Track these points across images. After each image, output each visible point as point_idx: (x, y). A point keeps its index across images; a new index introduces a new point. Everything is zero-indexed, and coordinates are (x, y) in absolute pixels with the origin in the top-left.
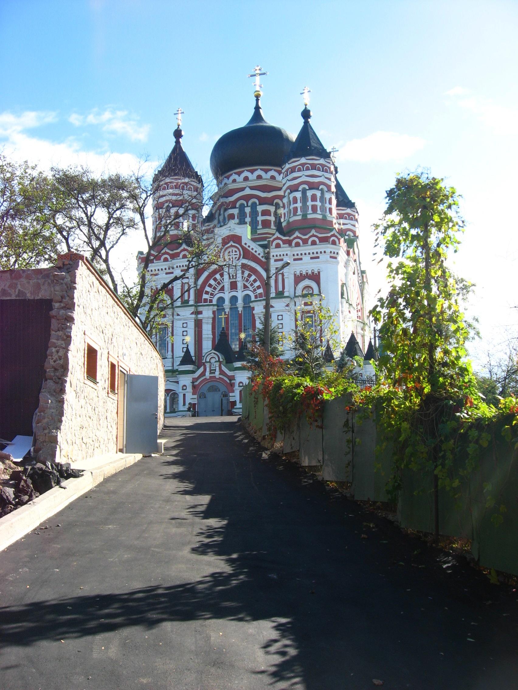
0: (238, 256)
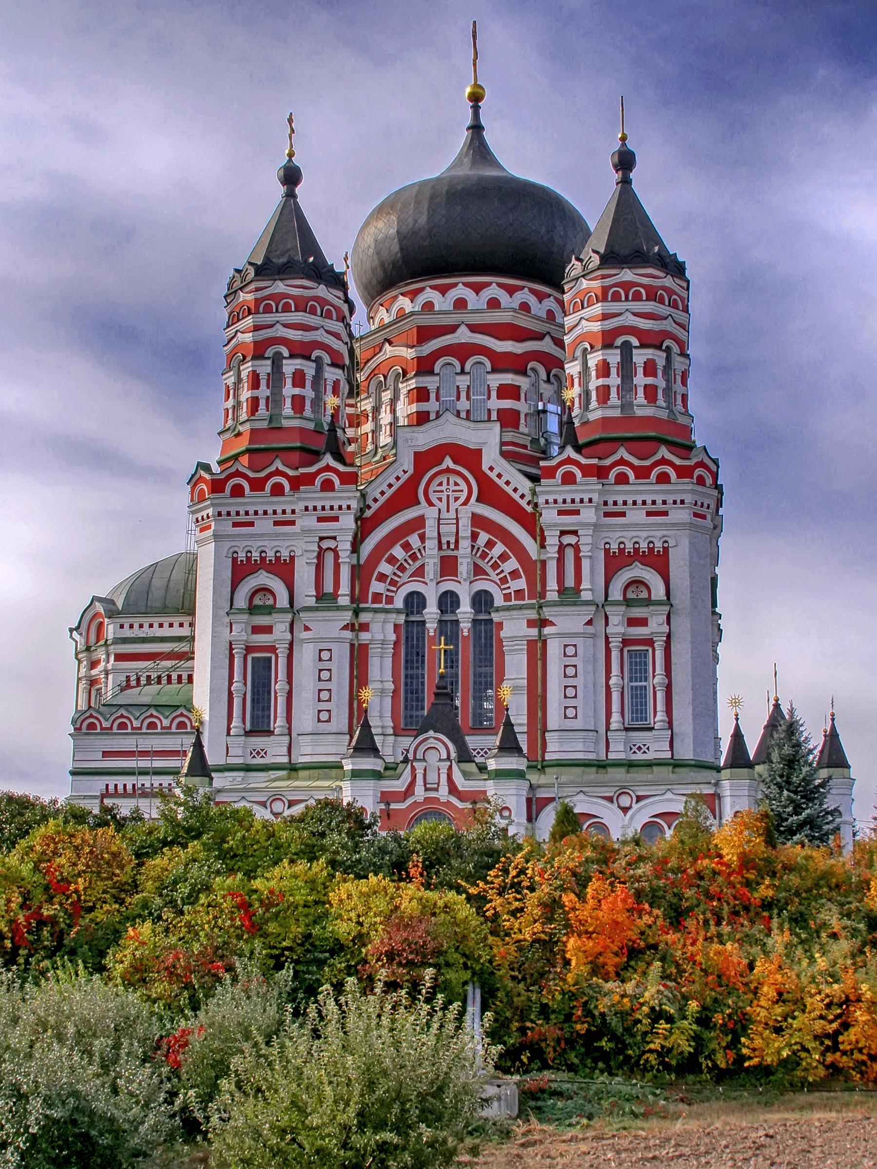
0: (463, 496)
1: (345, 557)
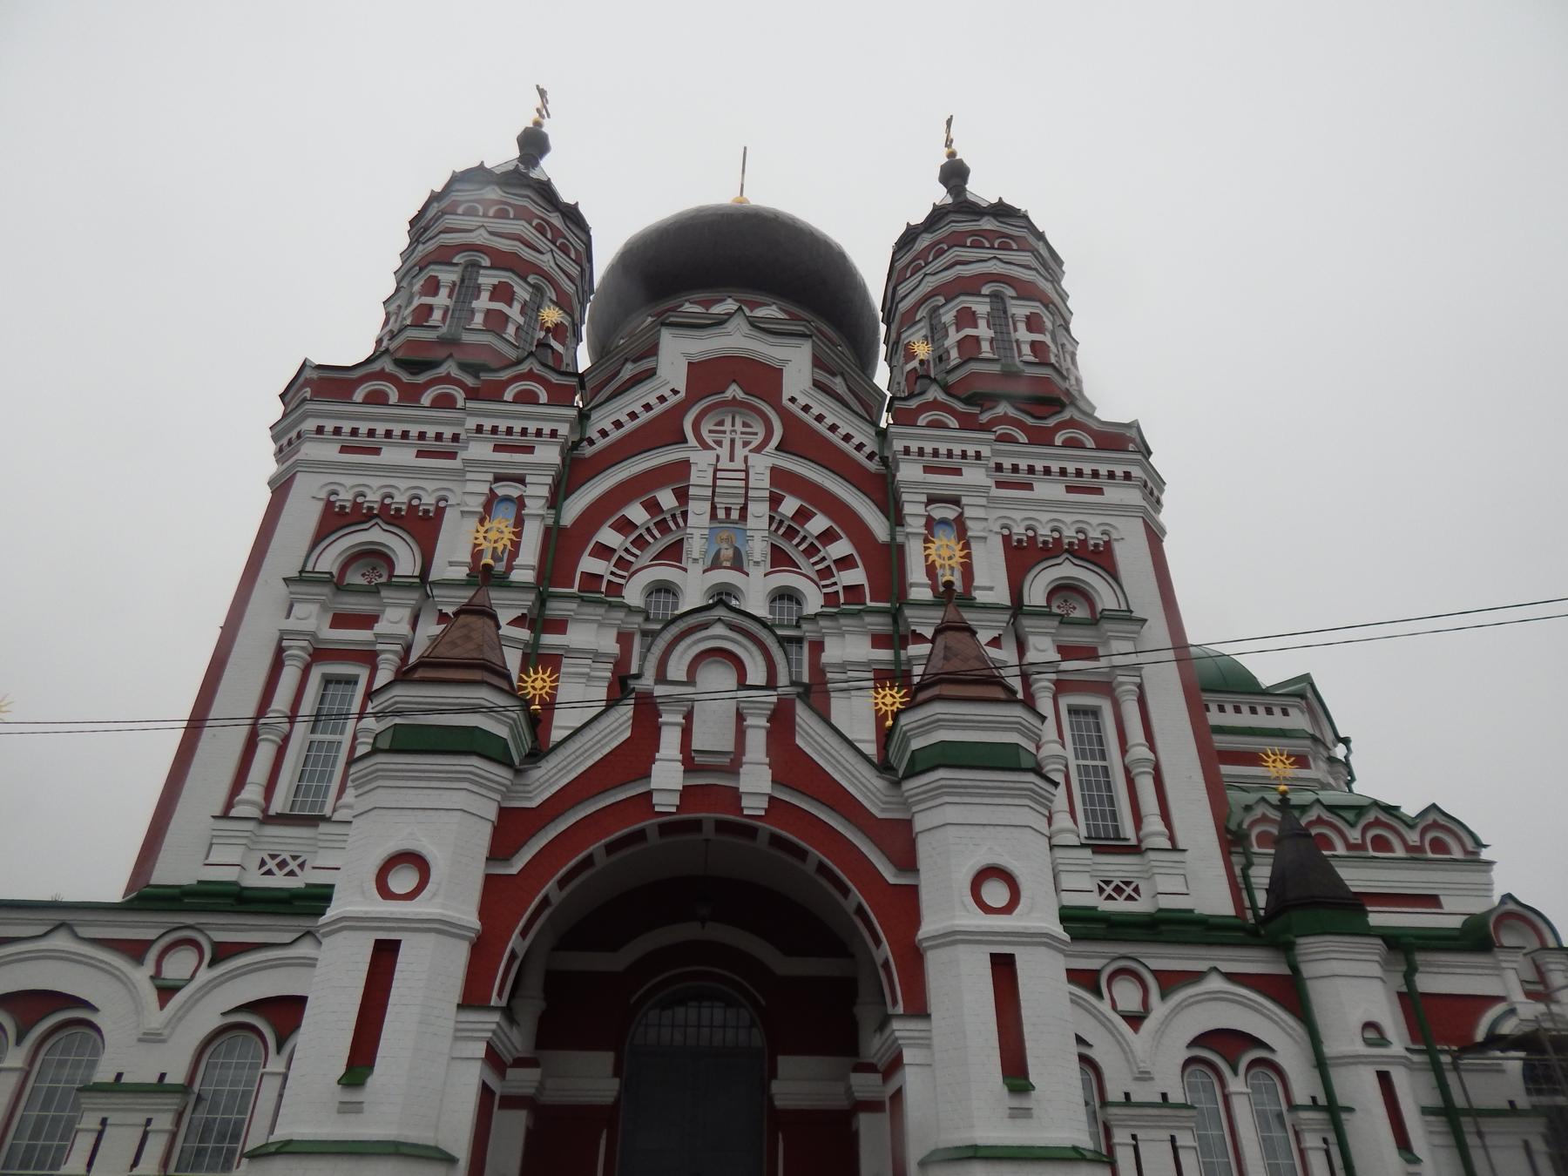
1: (535, 506)
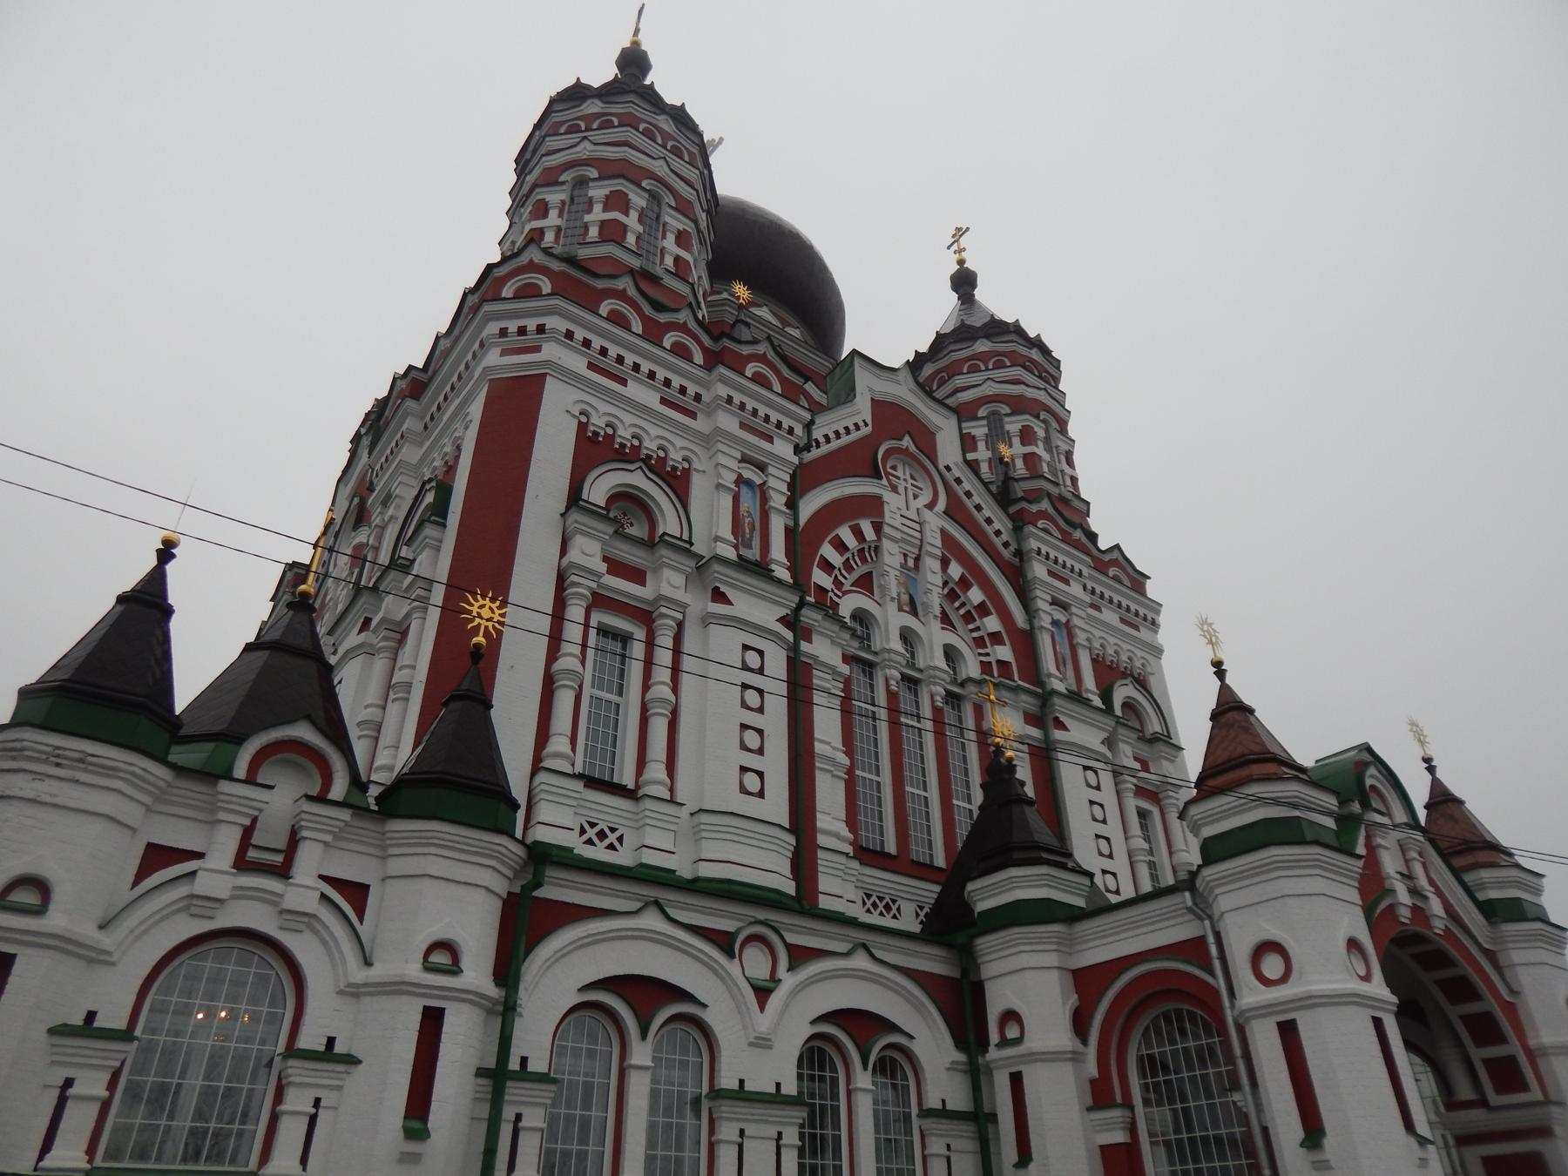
0: (925, 498)
